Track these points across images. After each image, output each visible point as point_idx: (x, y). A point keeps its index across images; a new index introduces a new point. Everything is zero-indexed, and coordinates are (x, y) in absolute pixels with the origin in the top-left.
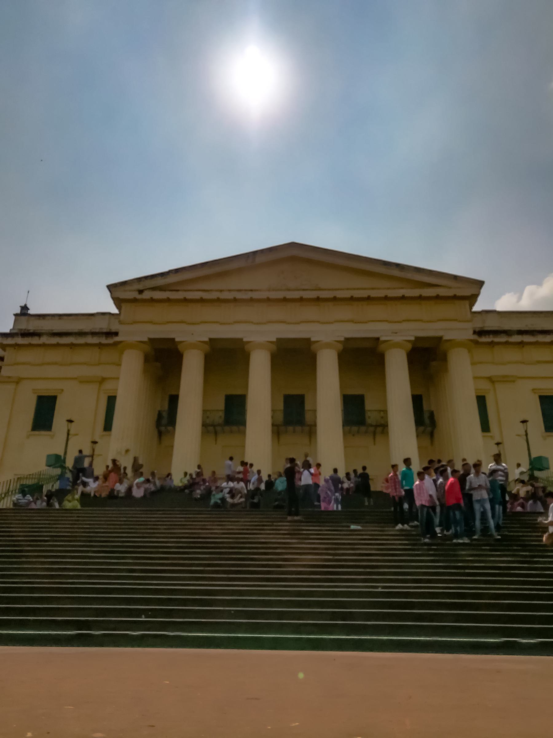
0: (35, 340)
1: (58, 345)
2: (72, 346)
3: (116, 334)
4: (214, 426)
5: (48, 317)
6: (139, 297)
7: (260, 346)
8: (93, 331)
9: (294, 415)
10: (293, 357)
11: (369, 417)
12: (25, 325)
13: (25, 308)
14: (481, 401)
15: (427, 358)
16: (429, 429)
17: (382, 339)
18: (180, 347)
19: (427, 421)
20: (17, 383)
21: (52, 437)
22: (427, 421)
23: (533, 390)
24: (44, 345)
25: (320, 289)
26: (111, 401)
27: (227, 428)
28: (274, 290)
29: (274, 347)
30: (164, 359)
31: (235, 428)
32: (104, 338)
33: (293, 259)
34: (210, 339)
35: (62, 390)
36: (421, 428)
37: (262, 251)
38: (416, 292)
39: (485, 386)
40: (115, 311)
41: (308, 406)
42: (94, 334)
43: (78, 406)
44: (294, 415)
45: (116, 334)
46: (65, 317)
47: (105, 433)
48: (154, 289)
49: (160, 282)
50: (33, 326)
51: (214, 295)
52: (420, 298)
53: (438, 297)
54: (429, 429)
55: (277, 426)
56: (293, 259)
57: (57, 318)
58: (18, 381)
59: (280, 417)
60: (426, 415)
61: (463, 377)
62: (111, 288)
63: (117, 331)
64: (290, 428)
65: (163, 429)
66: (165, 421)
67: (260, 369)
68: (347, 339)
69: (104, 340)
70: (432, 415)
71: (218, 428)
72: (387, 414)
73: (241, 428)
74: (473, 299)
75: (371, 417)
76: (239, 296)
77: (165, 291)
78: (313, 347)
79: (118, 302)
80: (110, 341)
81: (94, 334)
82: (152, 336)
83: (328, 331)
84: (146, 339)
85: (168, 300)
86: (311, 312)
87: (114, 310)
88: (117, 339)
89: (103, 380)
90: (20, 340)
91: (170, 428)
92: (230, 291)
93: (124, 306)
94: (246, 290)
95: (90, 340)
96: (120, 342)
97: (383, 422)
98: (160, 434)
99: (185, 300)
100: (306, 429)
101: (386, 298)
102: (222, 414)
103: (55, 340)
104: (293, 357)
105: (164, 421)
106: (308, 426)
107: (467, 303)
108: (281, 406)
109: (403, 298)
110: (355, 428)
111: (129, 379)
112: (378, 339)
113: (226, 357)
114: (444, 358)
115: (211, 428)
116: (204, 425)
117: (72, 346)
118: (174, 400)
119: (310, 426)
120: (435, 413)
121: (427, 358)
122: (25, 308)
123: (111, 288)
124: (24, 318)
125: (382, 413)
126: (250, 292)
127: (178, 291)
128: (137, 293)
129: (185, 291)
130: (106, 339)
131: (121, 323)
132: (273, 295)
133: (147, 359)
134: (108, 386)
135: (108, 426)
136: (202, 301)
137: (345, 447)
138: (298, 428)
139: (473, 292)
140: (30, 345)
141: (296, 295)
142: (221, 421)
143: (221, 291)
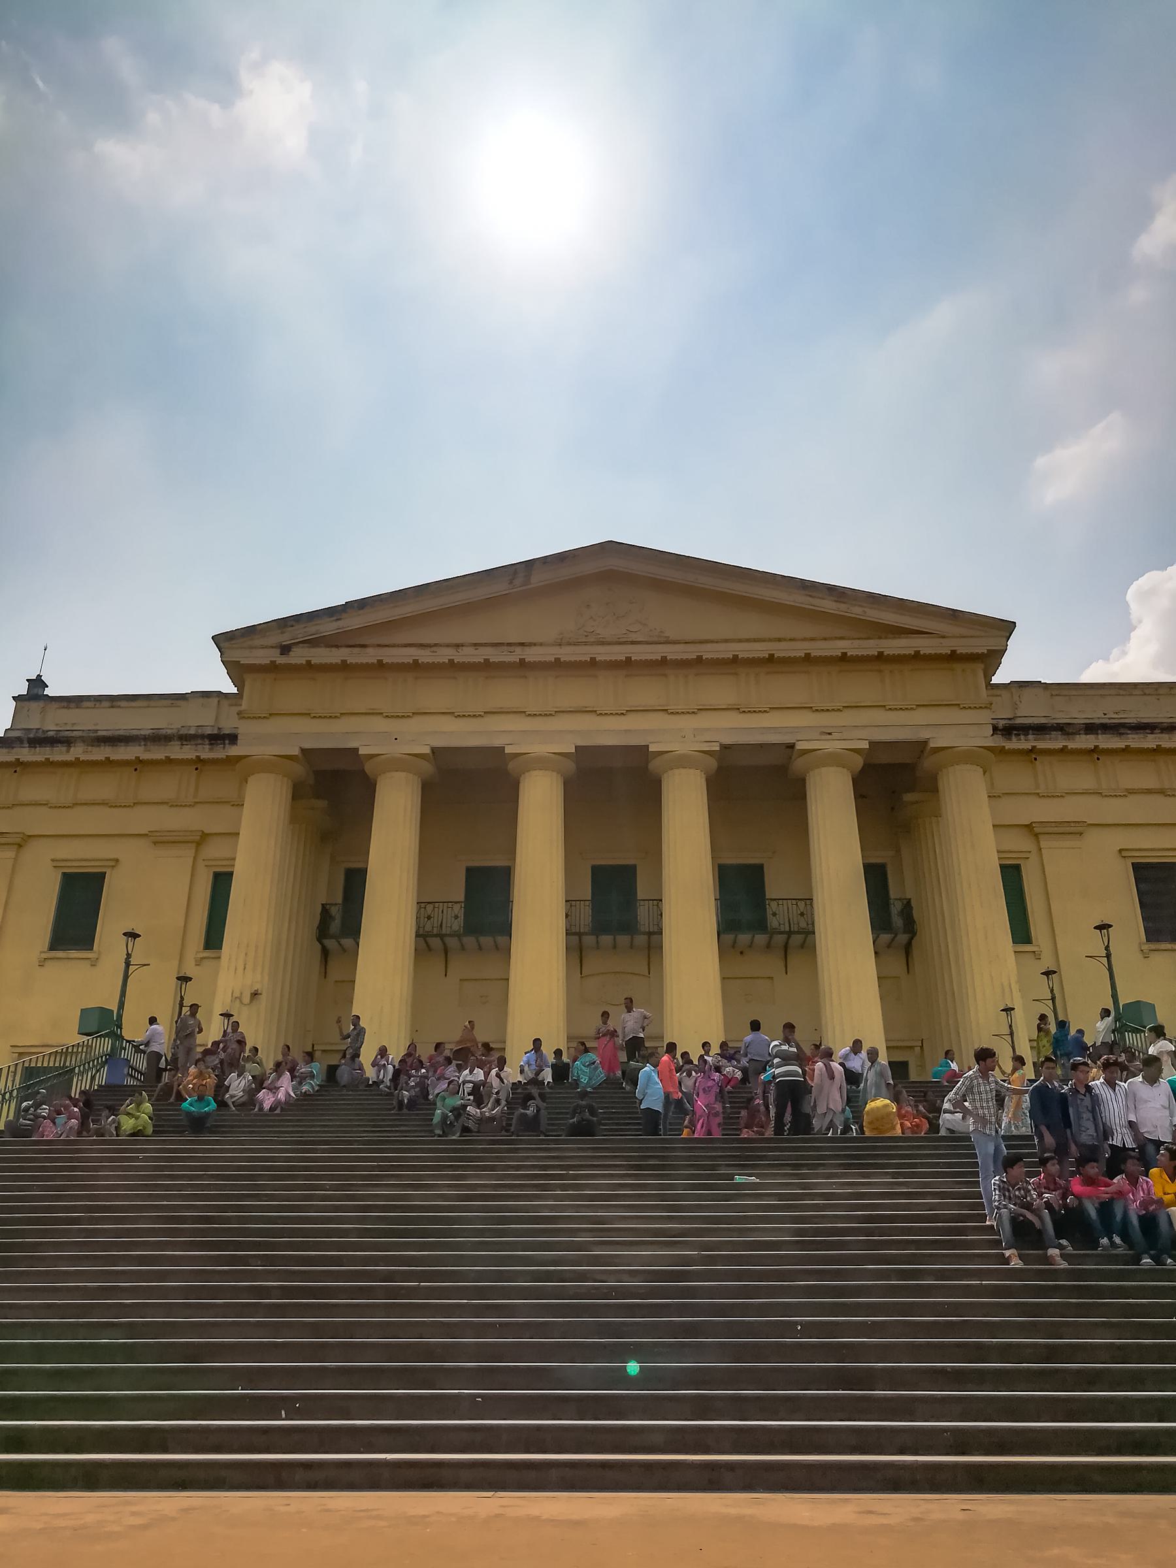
0: (59, 754)
1: (108, 762)
3: (233, 738)
4: (442, 936)
5: (86, 704)
6: (282, 660)
7: (541, 763)
8: (183, 732)
9: (614, 911)
10: (612, 788)
11: (774, 914)
12: (38, 721)
13: (37, 683)
14: (1012, 875)
15: (895, 788)
16: (903, 938)
17: (800, 746)
18: (368, 768)
19: (898, 922)
20: (20, 846)
21: (94, 963)
22: (898, 922)
23: (1120, 851)
24: (77, 763)
25: (668, 642)
26: (222, 882)
27: (469, 941)
28: (569, 644)
29: (571, 766)
30: (333, 793)
31: (486, 940)
33: (608, 578)
34: (434, 750)
35: (117, 860)
36: (885, 938)
37: (545, 560)
38: (870, 647)
39: (1020, 843)
40: (229, 687)
41: (642, 891)
42: (185, 739)
43: (150, 896)
44: (614, 911)
45: (233, 738)
46: (123, 704)
47: (207, 954)
48: (312, 643)
49: (328, 628)
50: (53, 722)
51: (443, 656)
52: (880, 657)
53: (917, 657)
54: (903, 938)
55: (580, 935)
57: (106, 704)
58: (21, 842)
59: (585, 915)
60: (896, 908)
61: (971, 830)
62: (223, 641)
63: (233, 731)
64: (606, 939)
65: (330, 944)
66: (335, 927)
67: (540, 810)
68: (725, 747)
69: (206, 753)
70: (907, 906)
71: (452, 942)
72: (811, 904)
73: (501, 939)
74: (993, 658)
75: (779, 916)
76: (496, 656)
77: (337, 646)
78: (654, 765)
79: (235, 670)
80: (220, 753)
81: (185, 739)
82: (307, 745)
83: (684, 730)
84: (295, 751)
85: (344, 667)
86: (646, 691)
87: (229, 687)
88: (234, 751)
89: (202, 839)
90: (25, 754)
91: (347, 942)
92: (475, 645)
93: (249, 680)
94: (509, 644)
95: (177, 752)
96: (240, 758)
97: (803, 925)
98: (325, 953)
99: (381, 665)
100: (641, 940)
101: (808, 659)
102: (457, 908)
103: (100, 753)
104: (612, 788)
105: (335, 926)
106: (644, 933)
107: (979, 668)
108: (586, 891)
109: (844, 658)
110: (744, 938)
111: (260, 837)
112: (791, 746)
113: (468, 789)
114: (932, 786)
115: (435, 943)
116: (422, 935)
117: (138, 764)
118: (355, 882)
119: (650, 934)
120: (913, 903)
121: (895, 788)
122: (37, 683)
123: (223, 641)
124: (35, 706)
125: (801, 904)
126: (518, 650)
129: (379, 646)
131: (241, 715)
132: (568, 654)
133: (298, 793)
134: (214, 851)
135: (213, 939)
136: (415, 666)
137: (724, 979)
138: (623, 939)
140: (48, 763)
141: (618, 653)
142: (457, 925)
143: (458, 646)
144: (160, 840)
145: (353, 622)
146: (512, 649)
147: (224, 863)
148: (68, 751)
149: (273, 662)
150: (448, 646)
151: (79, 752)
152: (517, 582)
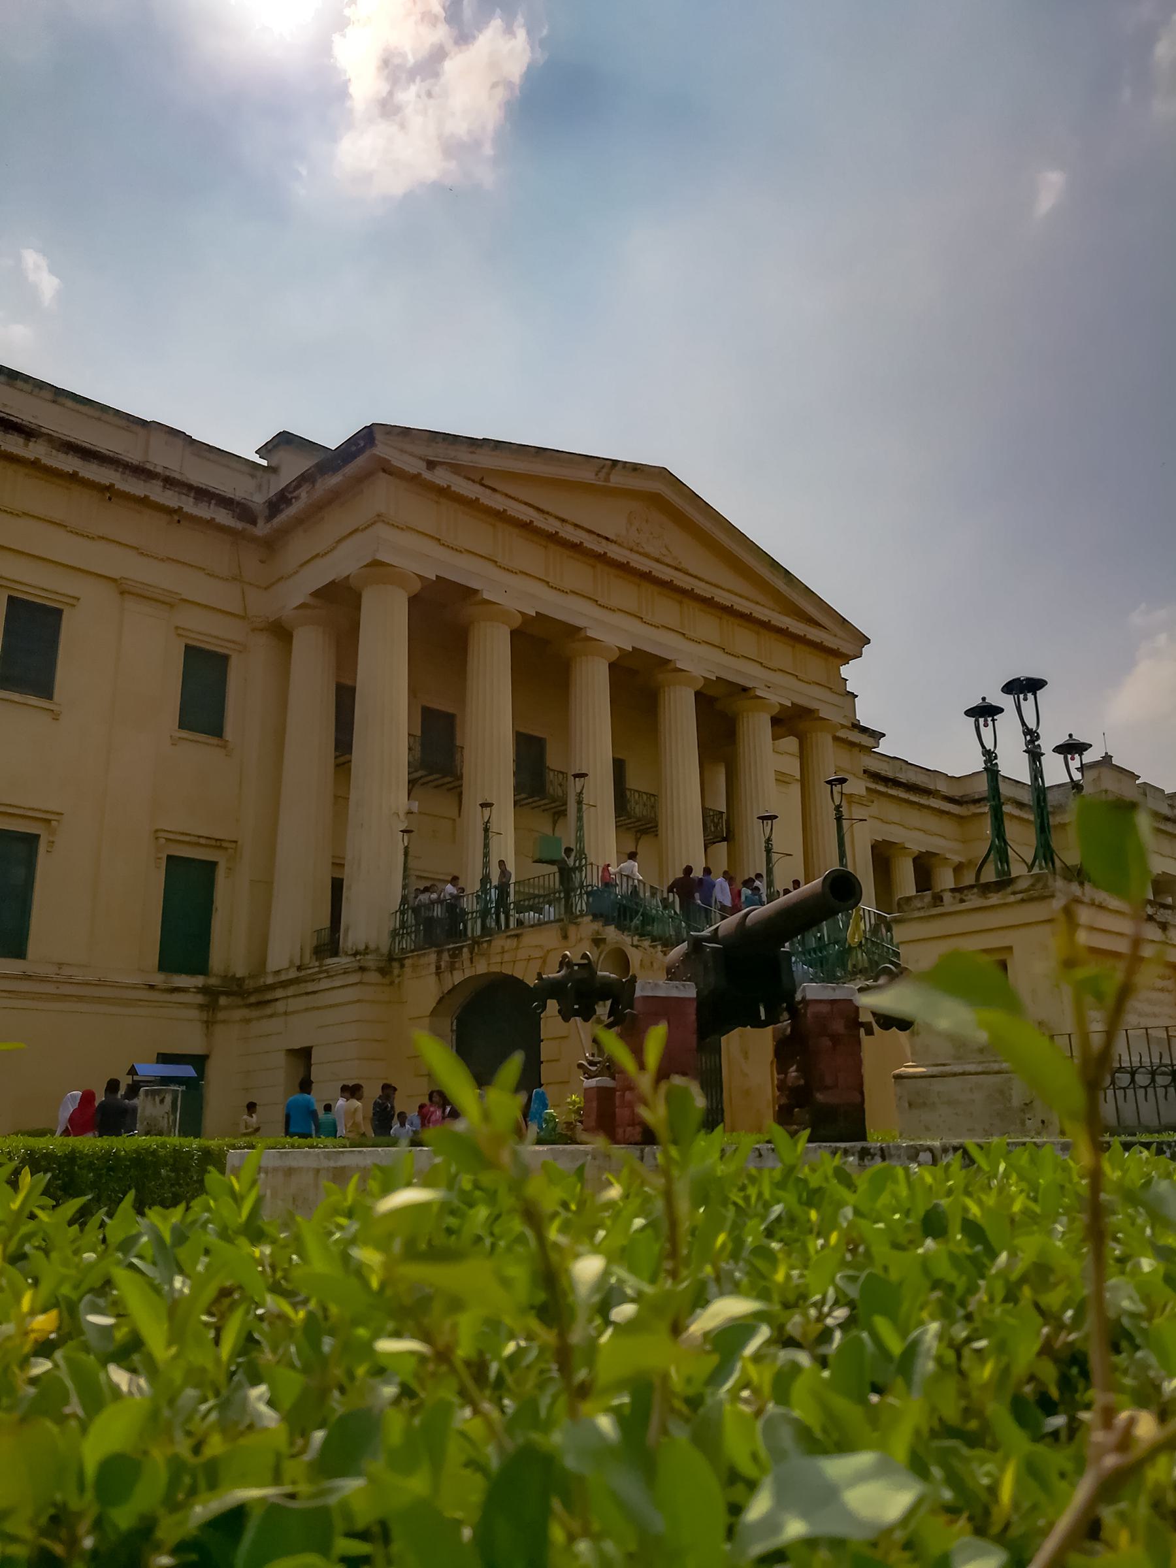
2: (108, 492)
5: (19, 384)
6: (427, 475)
24: (35, 465)
32: (191, 500)
46: (69, 403)
48: (456, 468)
51: (551, 526)
56: (656, 500)
74: (846, 659)
76: (590, 543)
92: (576, 526)
94: (599, 535)
103: (68, 463)
126: (604, 541)
127: (494, 490)
128: (424, 465)
130: (196, 504)
139: (846, 648)
143: (563, 521)
144: (124, 590)
145: (485, 460)
146: (600, 539)
147: (200, 637)
148: (26, 445)
149: (420, 474)
150: (557, 518)
151: (36, 450)
152: (602, 475)
